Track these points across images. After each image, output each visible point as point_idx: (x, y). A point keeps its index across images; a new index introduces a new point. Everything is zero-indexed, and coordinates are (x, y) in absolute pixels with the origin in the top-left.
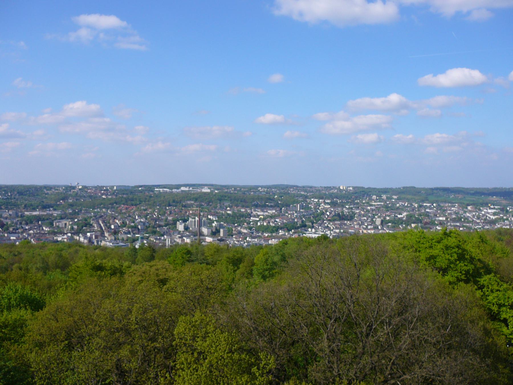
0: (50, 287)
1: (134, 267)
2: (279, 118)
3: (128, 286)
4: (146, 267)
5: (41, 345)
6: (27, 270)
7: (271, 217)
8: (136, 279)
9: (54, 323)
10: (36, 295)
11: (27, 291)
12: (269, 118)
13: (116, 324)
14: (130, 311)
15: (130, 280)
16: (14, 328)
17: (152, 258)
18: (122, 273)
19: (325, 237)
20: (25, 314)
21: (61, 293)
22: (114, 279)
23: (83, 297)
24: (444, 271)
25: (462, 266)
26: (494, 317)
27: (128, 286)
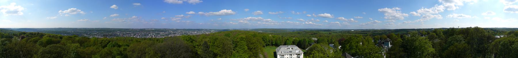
0: (130, 43)
1: (142, 41)
2: (165, 18)
3: (141, 44)
4: (144, 41)
5: (129, 52)
6: (127, 41)
7: (163, 33)
8: (142, 43)
9: (131, 49)
10: (128, 44)
11: (127, 44)
12: (163, 18)
13: (140, 50)
14: (141, 48)
15: (142, 43)
16: (125, 49)
17: (145, 40)
18: (140, 42)
19: (171, 37)
20: (127, 47)
21: (132, 44)
22: (140, 43)
23: (135, 45)
24: (188, 41)
25: (191, 40)
26: (195, 47)
27: (141, 44)
